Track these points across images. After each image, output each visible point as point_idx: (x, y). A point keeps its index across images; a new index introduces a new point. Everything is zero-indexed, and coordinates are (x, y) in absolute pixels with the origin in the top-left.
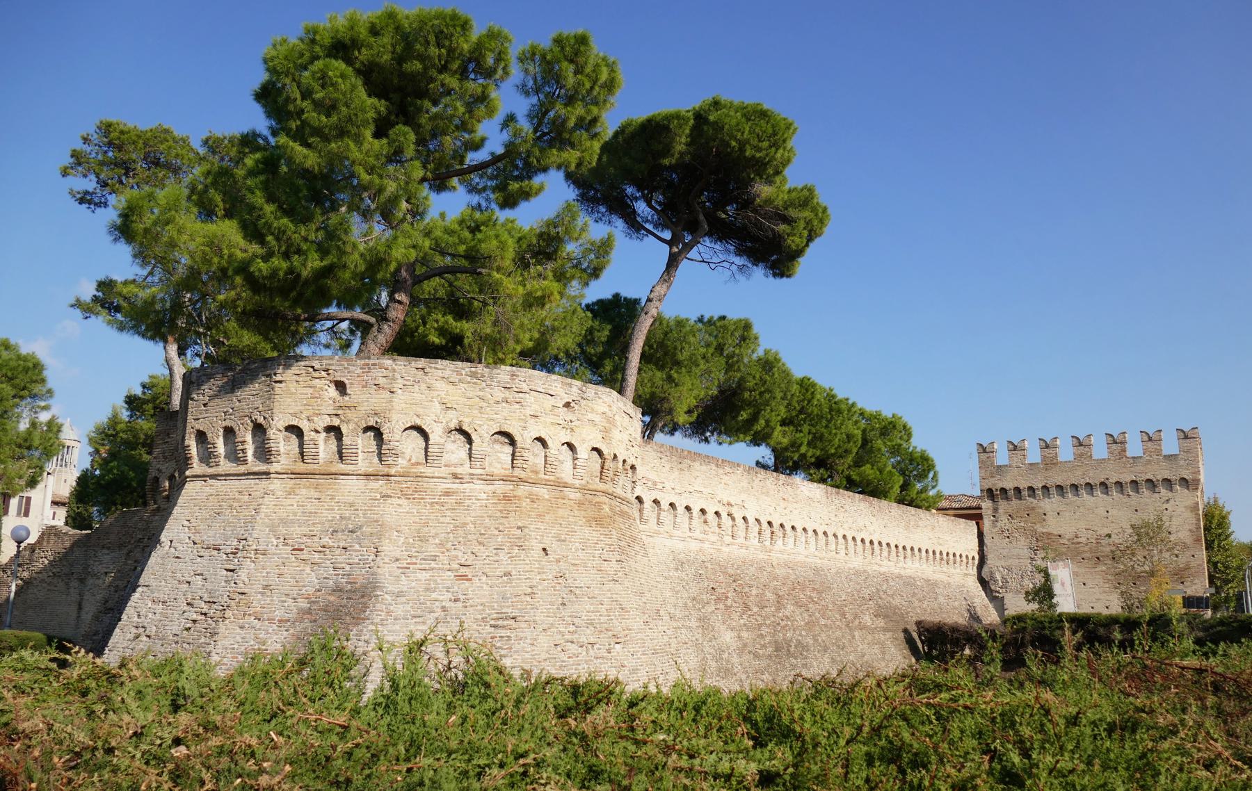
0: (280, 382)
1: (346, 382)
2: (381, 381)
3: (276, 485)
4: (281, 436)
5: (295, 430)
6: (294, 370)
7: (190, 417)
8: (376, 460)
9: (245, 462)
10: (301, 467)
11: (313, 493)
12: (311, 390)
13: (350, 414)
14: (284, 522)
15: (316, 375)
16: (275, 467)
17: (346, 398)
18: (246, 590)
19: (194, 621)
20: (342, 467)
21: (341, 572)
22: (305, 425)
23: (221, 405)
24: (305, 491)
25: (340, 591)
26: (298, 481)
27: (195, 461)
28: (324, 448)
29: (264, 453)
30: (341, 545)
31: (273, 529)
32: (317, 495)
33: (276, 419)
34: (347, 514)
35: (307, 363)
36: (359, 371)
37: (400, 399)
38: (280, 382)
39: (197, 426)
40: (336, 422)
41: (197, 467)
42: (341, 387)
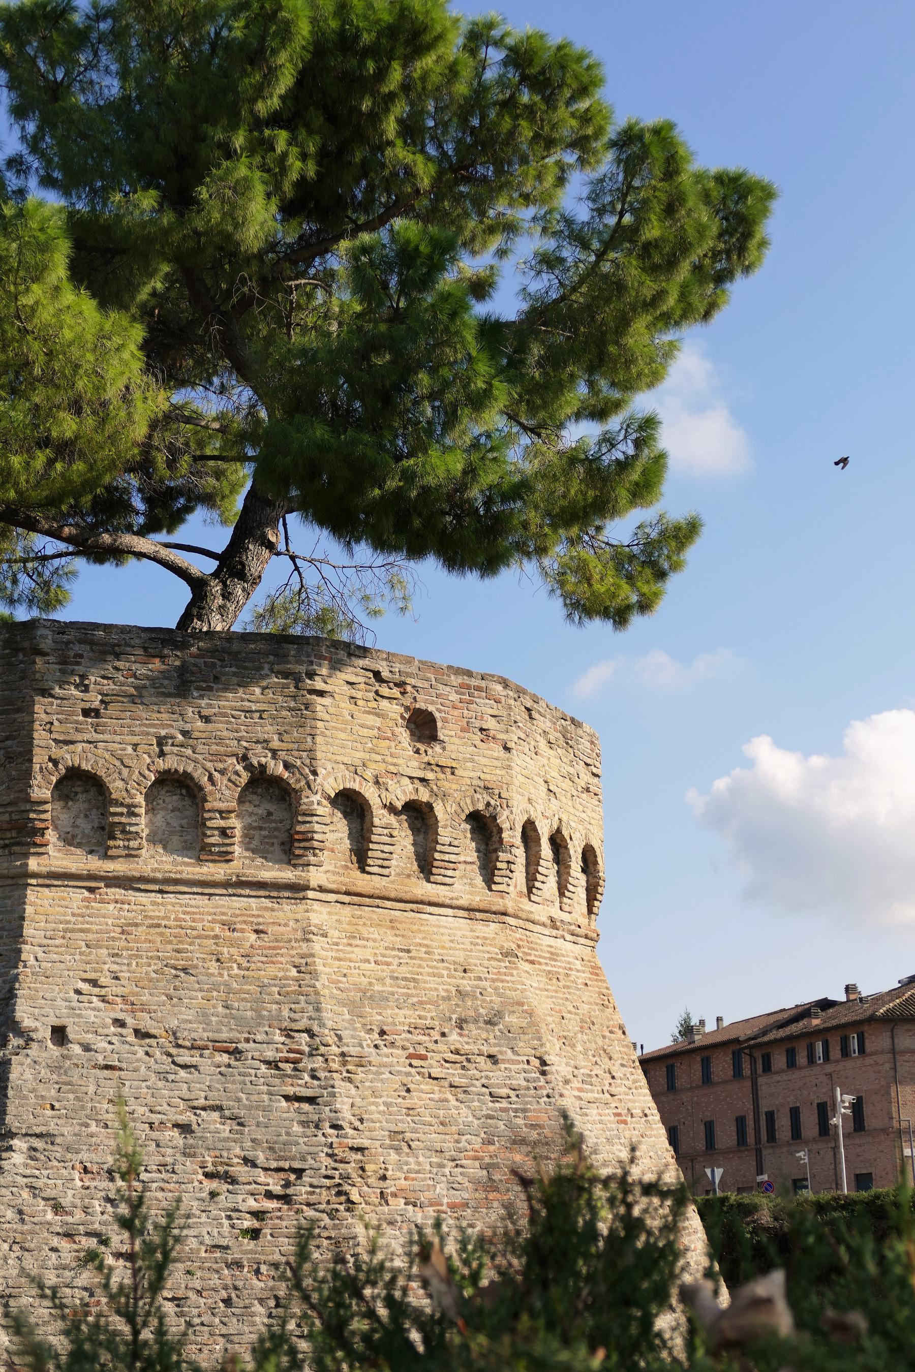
0: (321, 693)
1: (437, 715)
2: (491, 724)
3: (320, 914)
4: (324, 809)
5: (351, 804)
6: (348, 674)
7: (40, 736)
8: (479, 880)
9: (225, 857)
10: (362, 882)
11: (390, 938)
12: (377, 722)
13: (448, 784)
14: (368, 996)
15: (384, 690)
16: (316, 877)
17: (438, 748)
18: (366, 1143)
19: (258, 1215)
20: (423, 889)
21: (504, 1104)
22: (370, 793)
23: (160, 720)
24: (377, 931)
25: (524, 1141)
26: (358, 912)
27: (51, 836)
28: (396, 842)
29: (292, 844)
30: (485, 1049)
31: (355, 1009)
32: (399, 942)
33: (321, 771)
34: (466, 984)
35: (365, 662)
36: (454, 697)
37: (520, 761)
38: (321, 693)
39: (70, 757)
40: (424, 796)
41: (54, 855)
42: (423, 726)
